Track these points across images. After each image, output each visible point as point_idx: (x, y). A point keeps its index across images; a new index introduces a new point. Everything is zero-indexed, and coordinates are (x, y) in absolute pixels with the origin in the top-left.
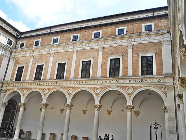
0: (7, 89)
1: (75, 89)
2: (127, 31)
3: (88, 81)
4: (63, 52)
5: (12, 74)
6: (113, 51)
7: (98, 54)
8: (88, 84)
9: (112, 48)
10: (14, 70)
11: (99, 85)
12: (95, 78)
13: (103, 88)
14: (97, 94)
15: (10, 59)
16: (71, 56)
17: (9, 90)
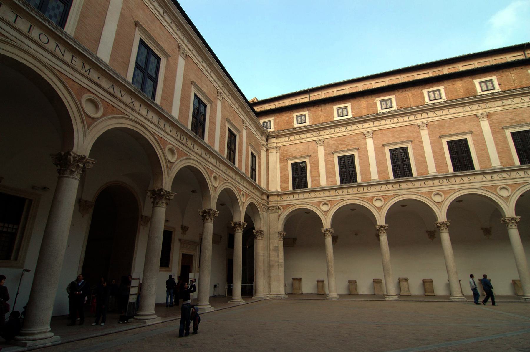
0: (281, 206)
1: (449, 193)
2: (500, 84)
3: (475, 177)
4: (394, 129)
5: (281, 177)
6: (511, 119)
7: (479, 126)
8: (476, 181)
9: (508, 112)
10: (283, 169)
11: (503, 181)
12: (425, 179)
13: (515, 185)
14: (506, 199)
15: (267, 150)
16: (415, 134)
17: (285, 207)
